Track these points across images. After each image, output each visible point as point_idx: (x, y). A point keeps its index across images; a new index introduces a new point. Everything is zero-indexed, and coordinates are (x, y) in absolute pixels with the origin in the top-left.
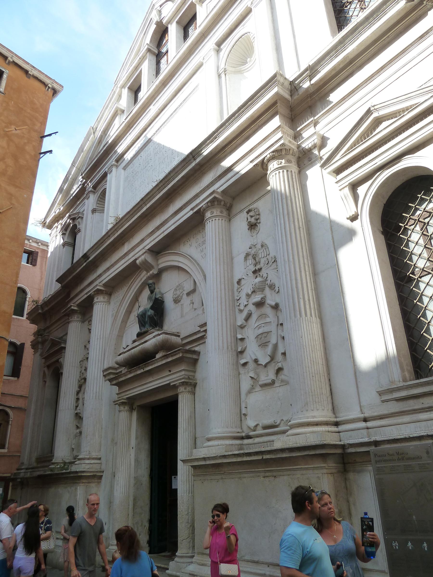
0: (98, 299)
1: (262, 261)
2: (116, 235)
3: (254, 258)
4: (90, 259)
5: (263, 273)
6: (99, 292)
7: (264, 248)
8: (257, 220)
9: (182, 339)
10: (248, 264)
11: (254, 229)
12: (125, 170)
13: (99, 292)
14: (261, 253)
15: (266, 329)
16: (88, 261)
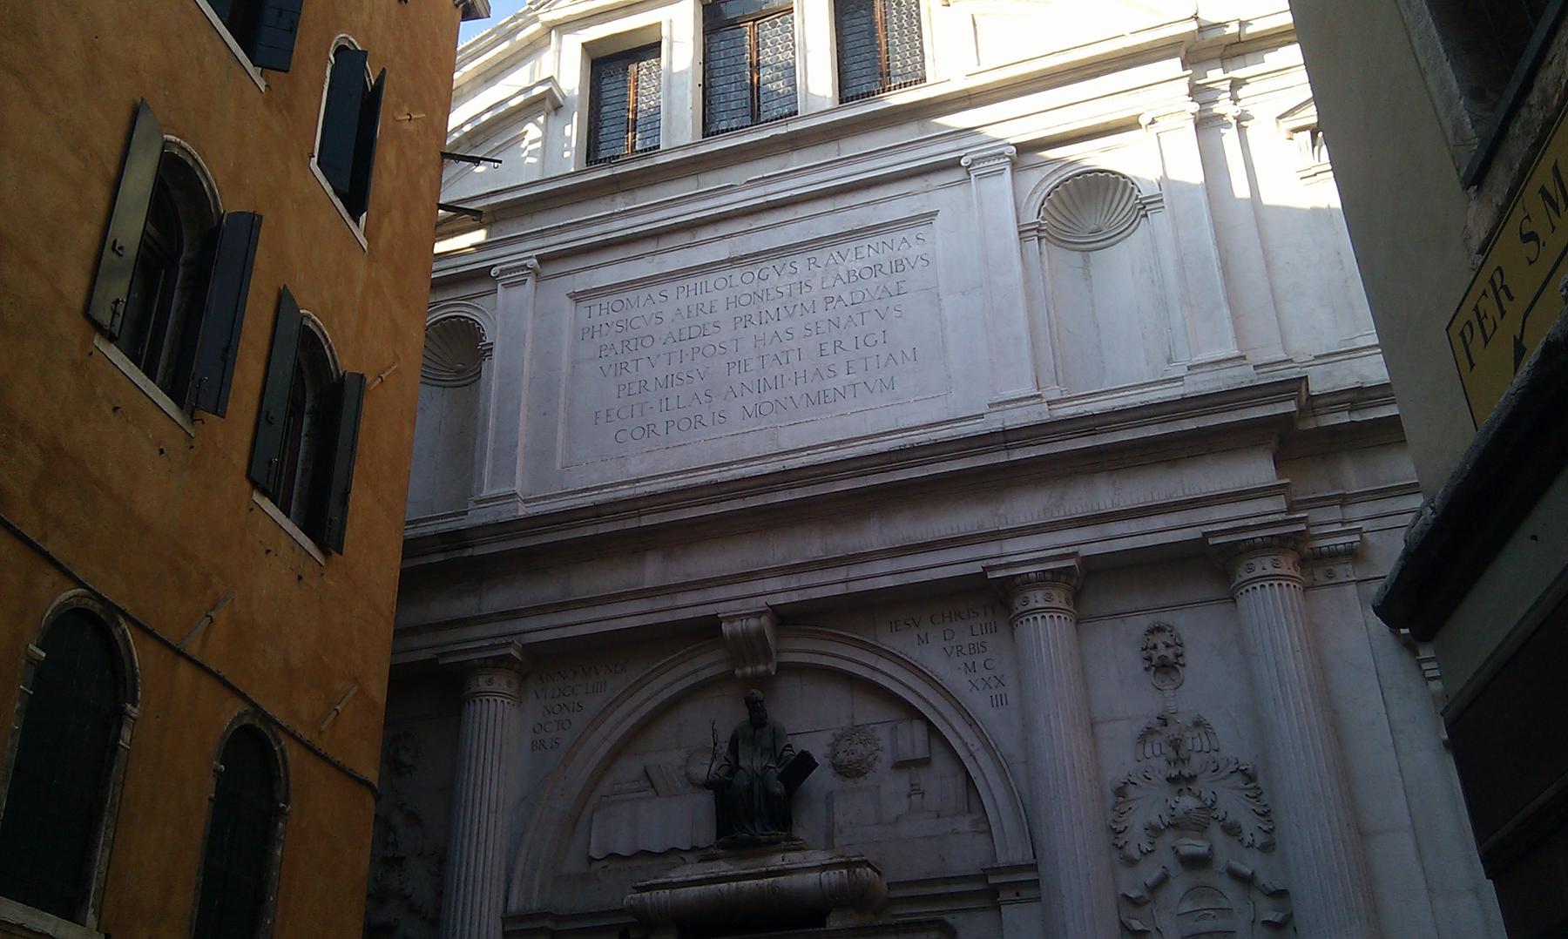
0: (490, 682)
1: (1196, 759)
2: (632, 524)
3: (1177, 749)
4: (468, 552)
5: (1200, 785)
6: (501, 663)
7: (1201, 731)
8: (1177, 656)
9: (891, 885)
10: (1148, 752)
11: (1167, 673)
12: (577, 301)
13: (501, 663)
14: (1194, 741)
15: (1222, 924)
16: (456, 554)
